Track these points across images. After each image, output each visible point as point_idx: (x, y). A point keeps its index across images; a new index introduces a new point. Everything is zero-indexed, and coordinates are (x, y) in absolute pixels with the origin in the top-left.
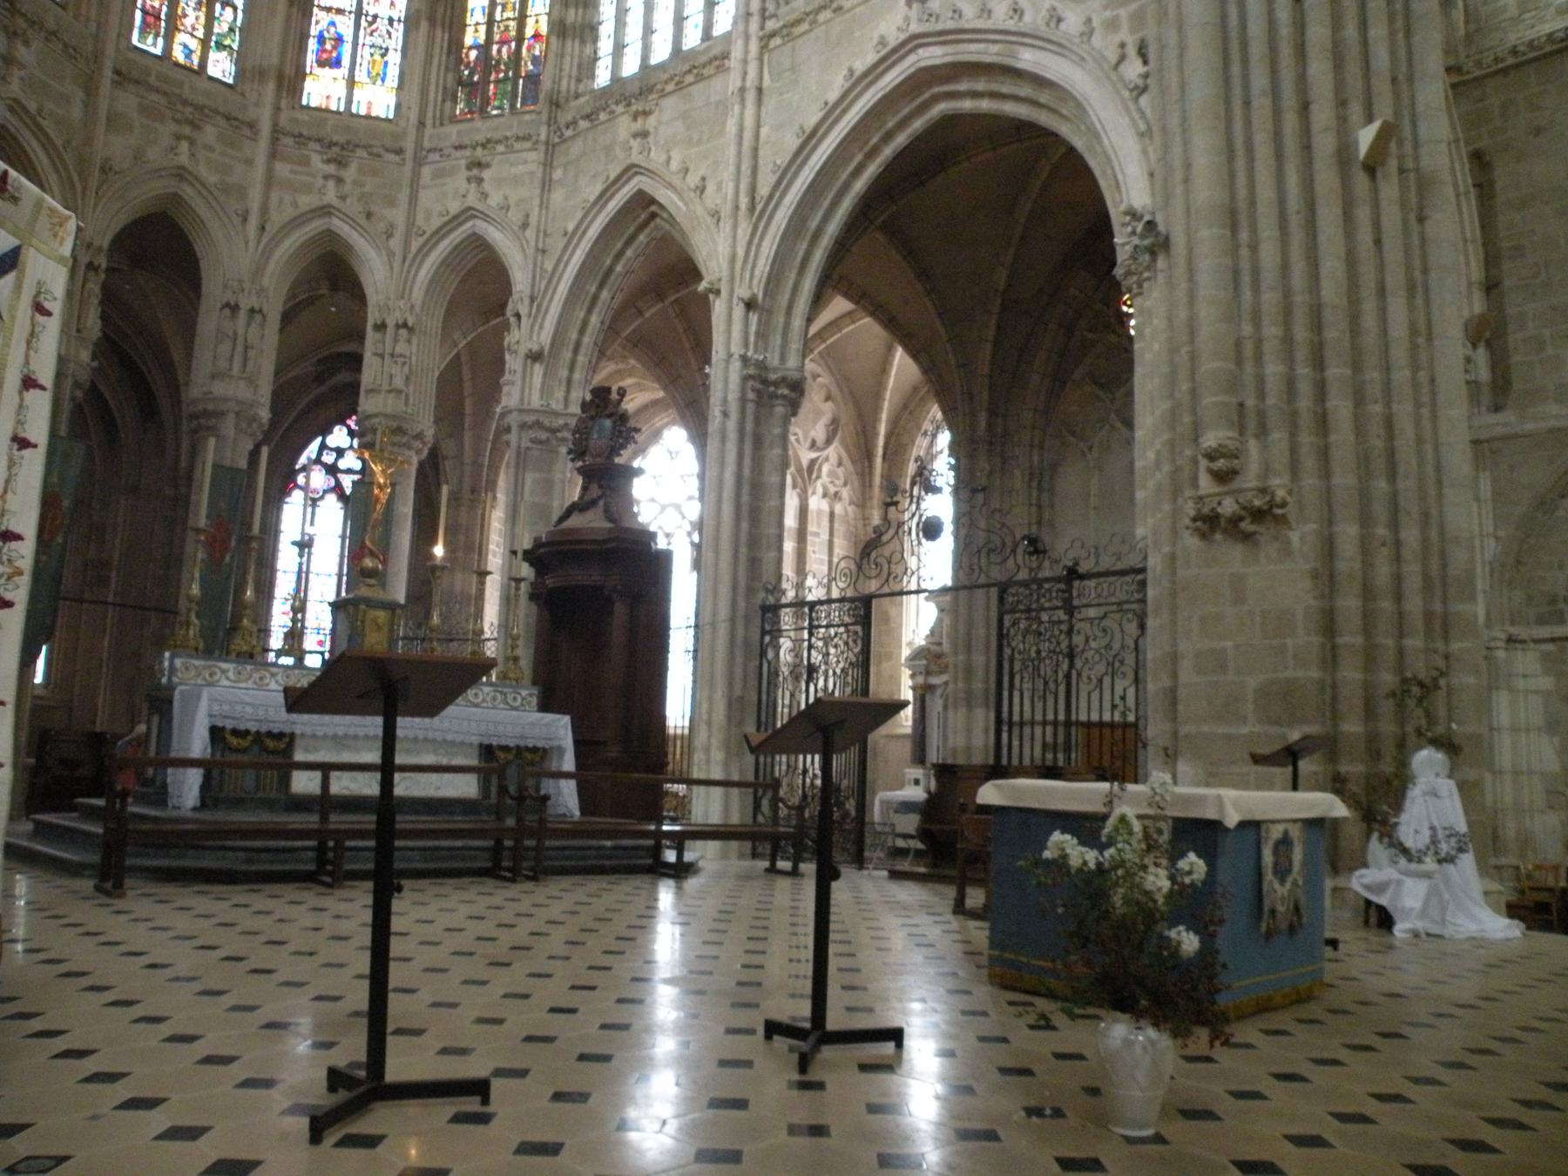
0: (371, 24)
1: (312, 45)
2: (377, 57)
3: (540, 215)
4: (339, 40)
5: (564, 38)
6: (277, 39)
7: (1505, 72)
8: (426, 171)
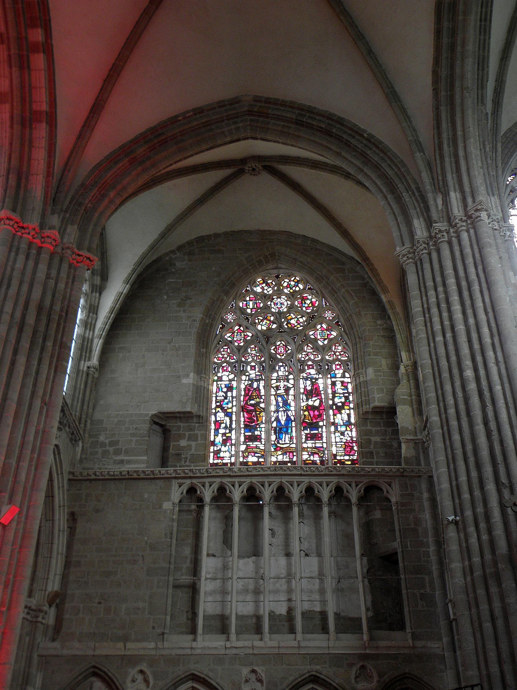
7: (91, 480)
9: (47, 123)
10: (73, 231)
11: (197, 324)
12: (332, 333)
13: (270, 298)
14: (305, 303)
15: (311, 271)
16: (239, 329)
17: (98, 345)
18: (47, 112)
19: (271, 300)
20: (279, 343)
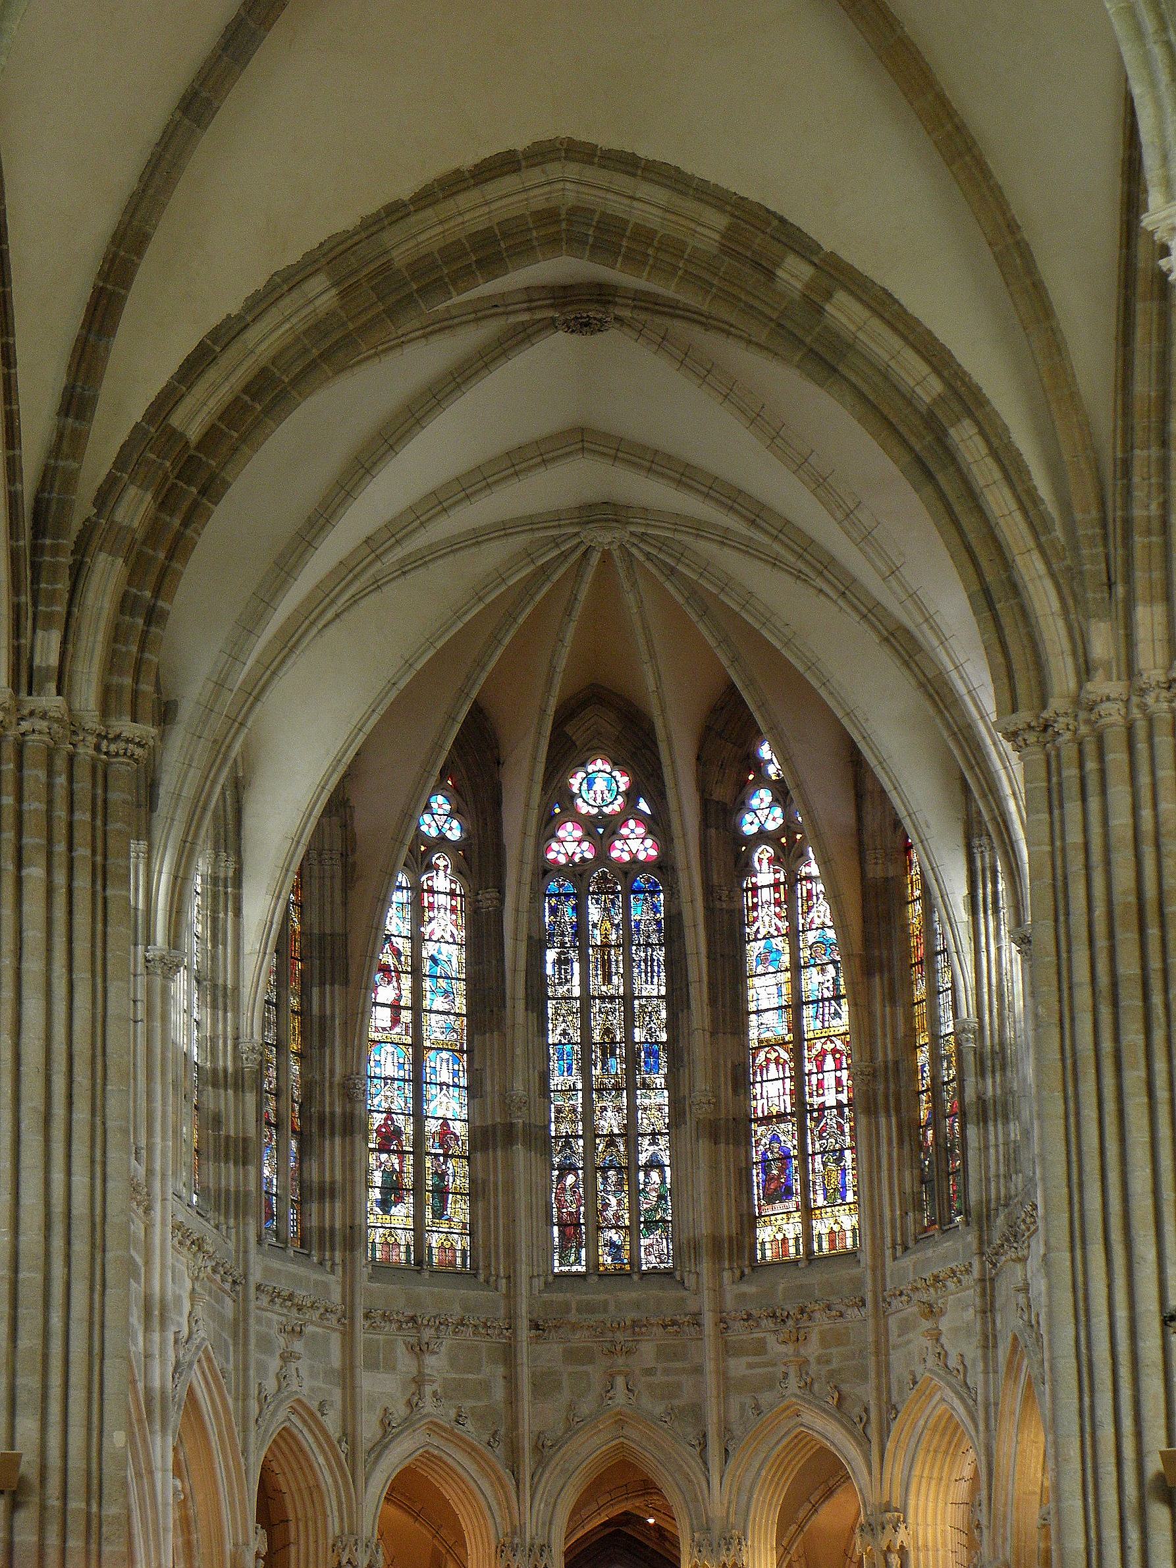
0: (817, 1121)
1: (757, 1176)
2: (832, 1166)
3: (986, 1383)
4: (786, 1157)
5: (985, 1122)
6: (703, 1201)
8: (893, 1323)
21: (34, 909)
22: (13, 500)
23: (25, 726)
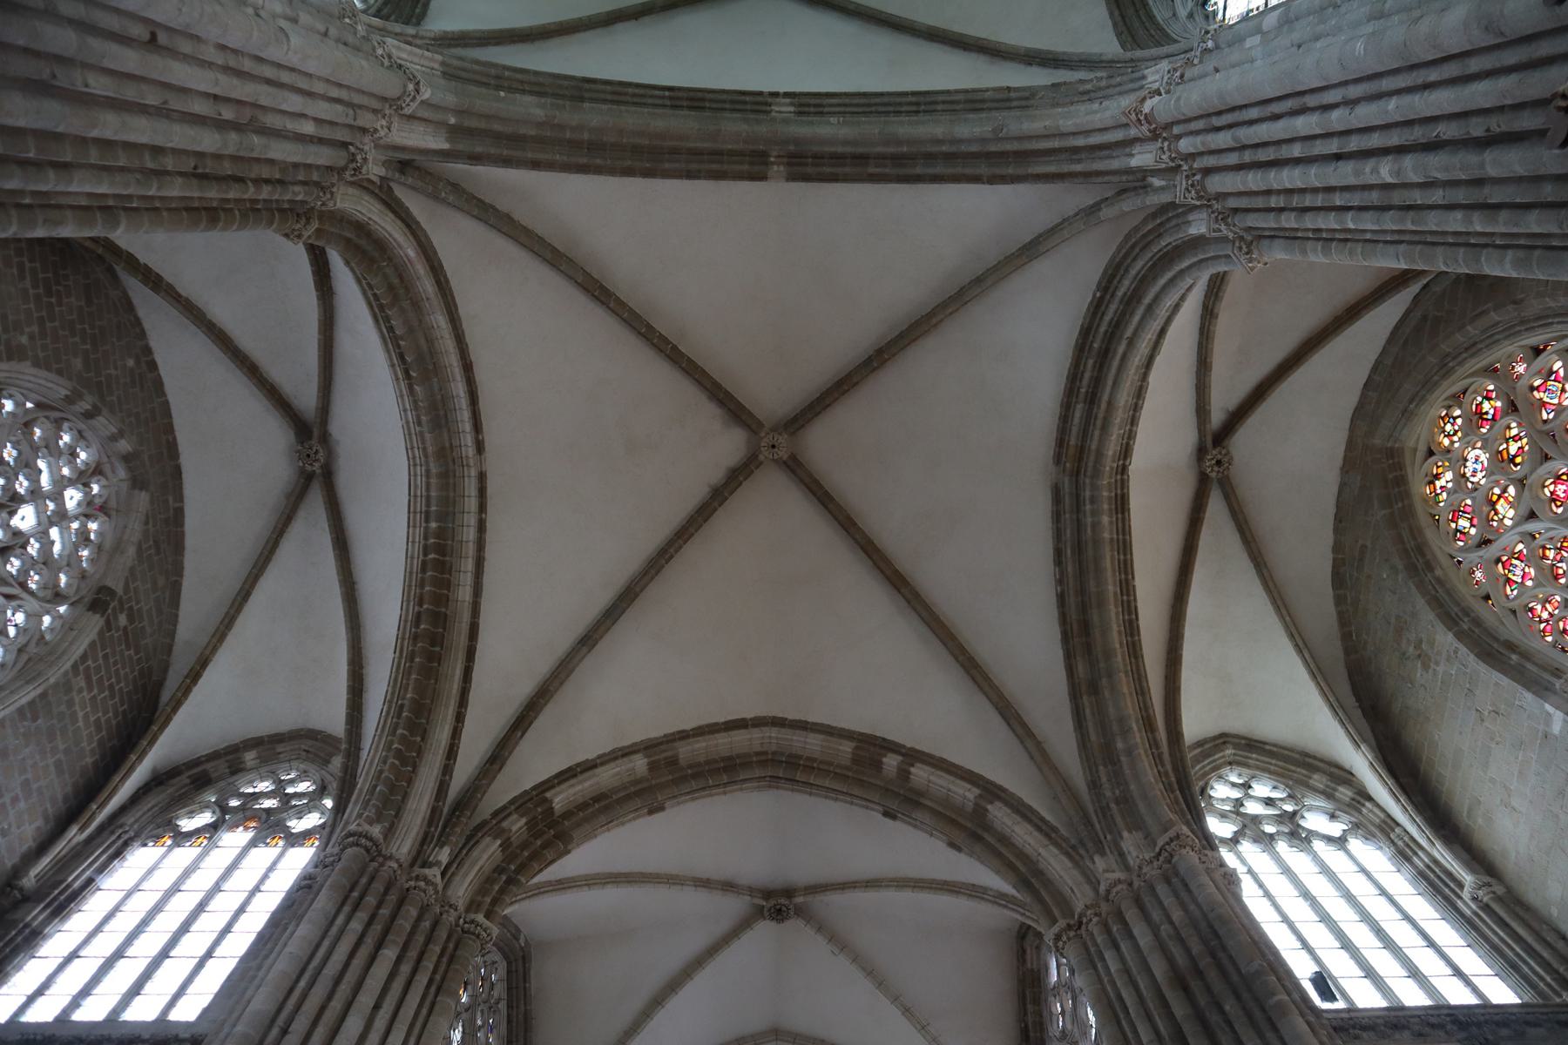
9: (991, 803)
10: (1130, 843)
11: (1463, 650)
12: (1555, 368)
13: (1461, 478)
14: (1487, 413)
15: (1428, 386)
16: (1503, 563)
17: (1442, 854)
18: (980, 796)
19: (1463, 480)
20: (1546, 490)
21: (380, 971)
22: (442, 788)
23: (412, 883)
